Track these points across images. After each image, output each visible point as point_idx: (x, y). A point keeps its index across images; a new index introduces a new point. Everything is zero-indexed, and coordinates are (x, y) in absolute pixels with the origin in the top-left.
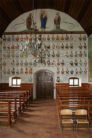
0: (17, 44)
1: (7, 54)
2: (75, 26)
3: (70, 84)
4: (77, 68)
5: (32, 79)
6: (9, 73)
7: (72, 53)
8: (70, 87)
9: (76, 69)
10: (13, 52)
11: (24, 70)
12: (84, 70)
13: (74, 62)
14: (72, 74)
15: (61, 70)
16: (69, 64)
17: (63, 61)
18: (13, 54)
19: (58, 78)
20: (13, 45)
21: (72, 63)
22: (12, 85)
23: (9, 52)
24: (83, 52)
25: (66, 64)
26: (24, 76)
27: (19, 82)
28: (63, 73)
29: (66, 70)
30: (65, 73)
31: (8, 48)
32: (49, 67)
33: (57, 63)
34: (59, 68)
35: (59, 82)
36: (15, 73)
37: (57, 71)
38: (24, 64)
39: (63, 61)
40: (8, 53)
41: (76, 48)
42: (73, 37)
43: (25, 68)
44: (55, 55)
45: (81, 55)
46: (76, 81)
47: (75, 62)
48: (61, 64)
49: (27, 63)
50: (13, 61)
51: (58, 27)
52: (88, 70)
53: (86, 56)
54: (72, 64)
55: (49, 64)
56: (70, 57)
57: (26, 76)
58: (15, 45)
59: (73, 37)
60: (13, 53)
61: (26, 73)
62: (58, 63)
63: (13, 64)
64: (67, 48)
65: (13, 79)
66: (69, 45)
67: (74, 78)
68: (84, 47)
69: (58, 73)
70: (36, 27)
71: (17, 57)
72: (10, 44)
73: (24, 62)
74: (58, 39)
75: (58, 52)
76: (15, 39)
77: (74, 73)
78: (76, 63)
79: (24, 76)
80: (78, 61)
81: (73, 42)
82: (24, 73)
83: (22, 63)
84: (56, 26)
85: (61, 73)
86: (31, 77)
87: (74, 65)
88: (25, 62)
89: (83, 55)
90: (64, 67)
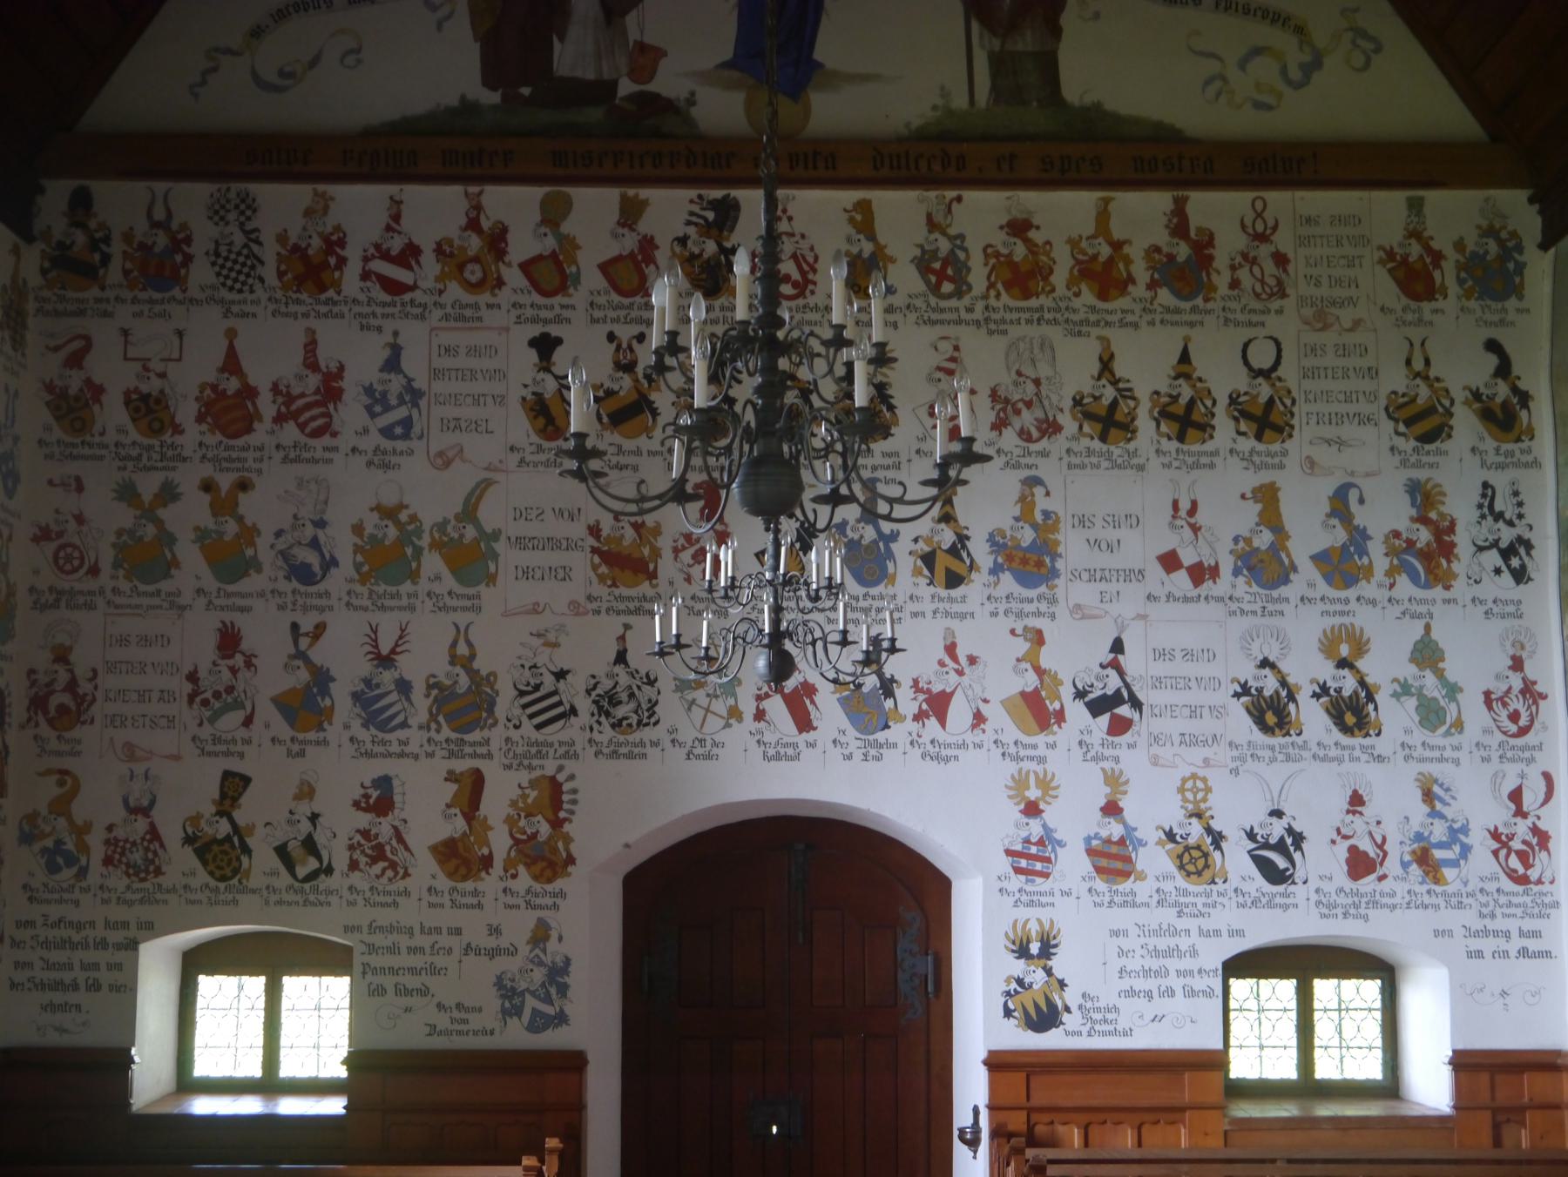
0: (311, 346)
1: (108, 518)
2: (1317, 63)
3: (1242, 1067)
4: (1371, 777)
5: (558, 975)
6: (137, 859)
7: (1271, 517)
8: (1246, 1110)
9: (1356, 800)
10: (225, 481)
11: (426, 814)
12: (1500, 814)
13: (1307, 667)
14: (1275, 876)
16: (1217, 711)
17: (1118, 647)
18: (231, 527)
19: (1022, 952)
20: (231, 364)
22: (187, 1084)
23: (148, 486)
24: (1461, 507)
26: (410, 913)
27: (319, 1026)
28: (1112, 860)
29: (1172, 813)
30: (1154, 860)
31: (149, 410)
32: (874, 752)
33: (1003, 680)
34: (1046, 784)
36: (263, 860)
37: (1009, 826)
38: (421, 704)
39: (1118, 647)
40: (127, 493)
41: (1348, 431)
42: (1284, 240)
43: (442, 765)
44: (979, 549)
46: (1348, 1003)
47: (1325, 670)
48: (1077, 712)
49: (483, 686)
50: (229, 641)
51: (1028, 74)
53: (1520, 576)
54: (1272, 713)
55: (870, 707)
57: (447, 917)
58: (272, 358)
59: (1284, 240)
60: (224, 506)
61: (460, 858)
62: (1030, 681)
63: (230, 698)
65: (203, 980)
66: (1222, 376)
67: (1302, 962)
68: (1487, 415)
69: (1031, 860)
70: (646, 58)
71: (303, 574)
72: (188, 346)
73: (425, 660)
74: (1023, 278)
75: (1026, 502)
76: (270, 252)
77: (1321, 862)
78: (1349, 685)
79: (410, 913)
80: (1385, 663)
81: (1286, 324)
82: (425, 868)
83: (387, 677)
84: (998, 63)
85: (1086, 865)
86: (540, 936)
87: (1312, 717)
88: (441, 668)
90: (1132, 756)
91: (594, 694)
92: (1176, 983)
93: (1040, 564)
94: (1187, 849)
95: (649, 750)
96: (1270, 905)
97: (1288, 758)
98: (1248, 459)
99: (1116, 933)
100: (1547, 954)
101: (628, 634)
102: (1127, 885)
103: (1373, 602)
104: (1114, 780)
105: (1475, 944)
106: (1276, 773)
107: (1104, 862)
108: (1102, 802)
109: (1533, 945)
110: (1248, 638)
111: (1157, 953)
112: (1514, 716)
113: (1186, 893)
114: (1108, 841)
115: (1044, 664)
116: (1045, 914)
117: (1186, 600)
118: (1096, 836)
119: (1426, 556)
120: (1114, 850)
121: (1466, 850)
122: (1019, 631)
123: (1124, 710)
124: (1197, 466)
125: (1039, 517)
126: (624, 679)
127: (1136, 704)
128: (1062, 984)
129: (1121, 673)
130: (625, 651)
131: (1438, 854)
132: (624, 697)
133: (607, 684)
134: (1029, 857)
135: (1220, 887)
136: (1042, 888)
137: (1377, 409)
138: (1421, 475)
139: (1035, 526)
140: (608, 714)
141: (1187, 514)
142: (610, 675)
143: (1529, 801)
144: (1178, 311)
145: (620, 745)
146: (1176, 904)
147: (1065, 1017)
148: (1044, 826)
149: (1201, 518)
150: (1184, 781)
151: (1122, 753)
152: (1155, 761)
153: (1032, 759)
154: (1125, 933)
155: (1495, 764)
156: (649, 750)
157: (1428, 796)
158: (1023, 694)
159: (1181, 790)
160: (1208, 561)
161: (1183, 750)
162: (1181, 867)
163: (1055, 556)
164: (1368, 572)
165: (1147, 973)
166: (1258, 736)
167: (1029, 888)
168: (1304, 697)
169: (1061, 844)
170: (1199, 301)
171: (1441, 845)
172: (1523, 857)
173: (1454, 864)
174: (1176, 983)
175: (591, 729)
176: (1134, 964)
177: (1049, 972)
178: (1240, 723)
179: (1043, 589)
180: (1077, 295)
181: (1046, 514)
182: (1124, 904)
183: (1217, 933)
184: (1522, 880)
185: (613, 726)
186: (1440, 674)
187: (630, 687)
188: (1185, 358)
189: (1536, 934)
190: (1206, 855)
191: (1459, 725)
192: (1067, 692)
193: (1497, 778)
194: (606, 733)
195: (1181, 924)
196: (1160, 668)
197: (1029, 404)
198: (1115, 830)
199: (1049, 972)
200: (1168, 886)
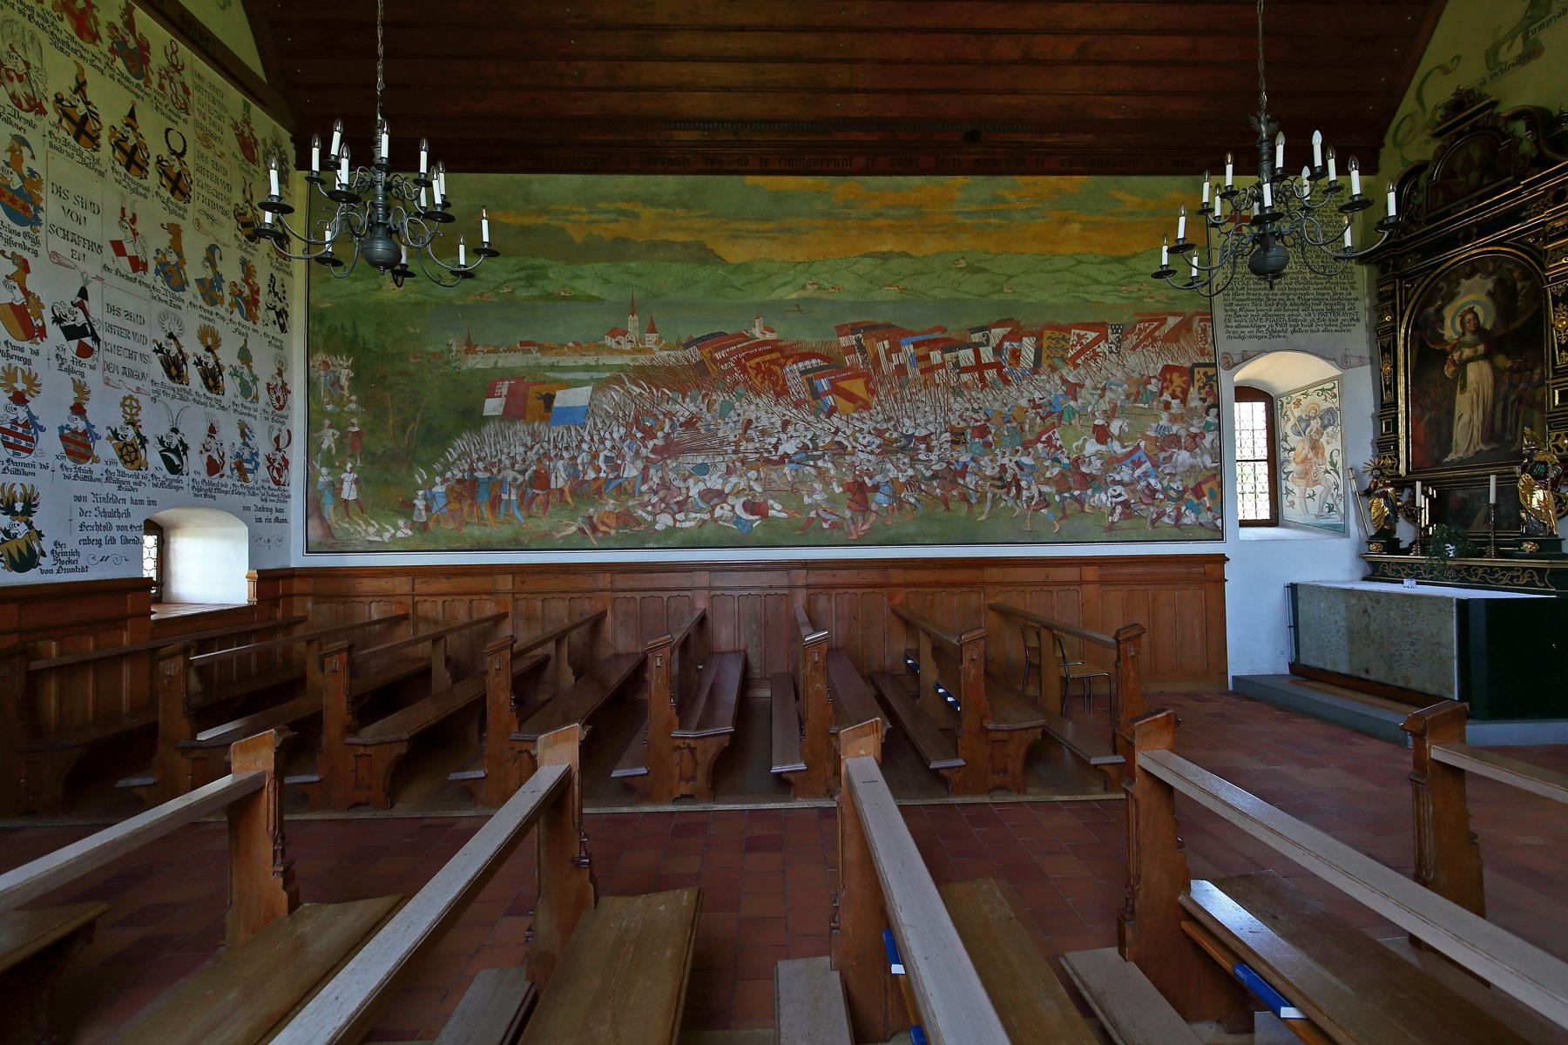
4: (221, 418)
7: (176, 245)
9: (212, 430)
13: (192, 347)
14: (174, 469)
15: (51, 409)
17: (83, 293)
21: (174, 351)
24: (262, 282)
25: (117, 349)
28: (78, 446)
30: (105, 450)
34: (31, 380)
35: (26, 561)
39: (83, 293)
45: (248, 304)
47: (201, 351)
48: (54, 332)
52: (297, 454)
53: (283, 328)
54: (174, 367)
56: (159, 283)
64: (132, 159)
77: (195, 463)
80: (227, 356)
85: (59, 448)
87: (193, 374)
89: (262, 305)
92: (116, 534)
93: (26, 209)
94: (126, 445)
96: (170, 487)
97: (182, 398)
98: (166, 202)
99: (78, 499)
100: (285, 521)
102: (86, 466)
103: (223, 318)
104: (80, 388)
105: (260, 515)
106: (176, 405)
107: (73, 447)
108: (72, 403)
109: (281, 516)
110: (163, 317)
111: (105, 514)
112: (278, 399)
113: (124, 475)
114: (75, 432)
115: (30, 287)
116: (27, 481)
117: (128, 278)
118: (67, 427)
119: (247, 303)
120: (79, 439)
121: (257, 464)
122: (8, 254)
123: (88, 340)
124: (135, 191)
125: (26, 173)
127: (96, 339)
128: (40, 535)
129: (86, 314)
131: (246, 466)
134: (16, 435)
135: (143, 473)
136: (26, 461)
137: (230, 208)
138: (248, 258)
139: (22, 177)
141: (129, 220)
143: (282, 443)
144: (128, 80)
146: (117, 481)
147: (42, 560)
148: (29, 413)
149: (138, 227)
150: (125, 399)
151: (86, 370)
152: (107, 382)
153: (19, 359)
154: (85, 499)
155: (269, 423)
157: (243, 434)
158: (11, 304)
159: (123, 405)
160: (142, 258)
161: (124, 378)
162: (121, 457)
163: (38, 209)
164: (222, 303)
165: (99, 527)
166: (167, 380)
167: (15, 460)
168: (190, 361)
169: (42, 429)
170: (141, 82)
171: (248, 461)
172: (279, 471)
173: (252, 471)
174: (116, 534)
176: (90, 521)
177: (30, 525)
178: (156, 369)
179: (27, 229)
180: (61, 20)
181: (30, 170)
182: (85, 478)
183: (141, 502)
184: (277, 483)
186: (250, 367)
188: (132, 115)
189: (281, 511)
190: (136, 451)
191: (256, 398)
192: (47, 316)
193: (271, 429)
195: (120, 494)
196: (111, 319)
197: (20, 78)
198: (81, 425)
199: (30, 525)
200: (113, 469)
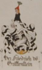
91: (6, 34)
95: (32, 62)
101: (20, 6)
126: (19, 28)
130: (19, 14)
132: (20, 36)
133: (11, 31)
140: (13, 44)
142: (13, 26)
145: (19, 59)
156: (32, 62)
175: (5, 51)
185: (16, 50)
187: (22, 32)
194: (12, 53)
